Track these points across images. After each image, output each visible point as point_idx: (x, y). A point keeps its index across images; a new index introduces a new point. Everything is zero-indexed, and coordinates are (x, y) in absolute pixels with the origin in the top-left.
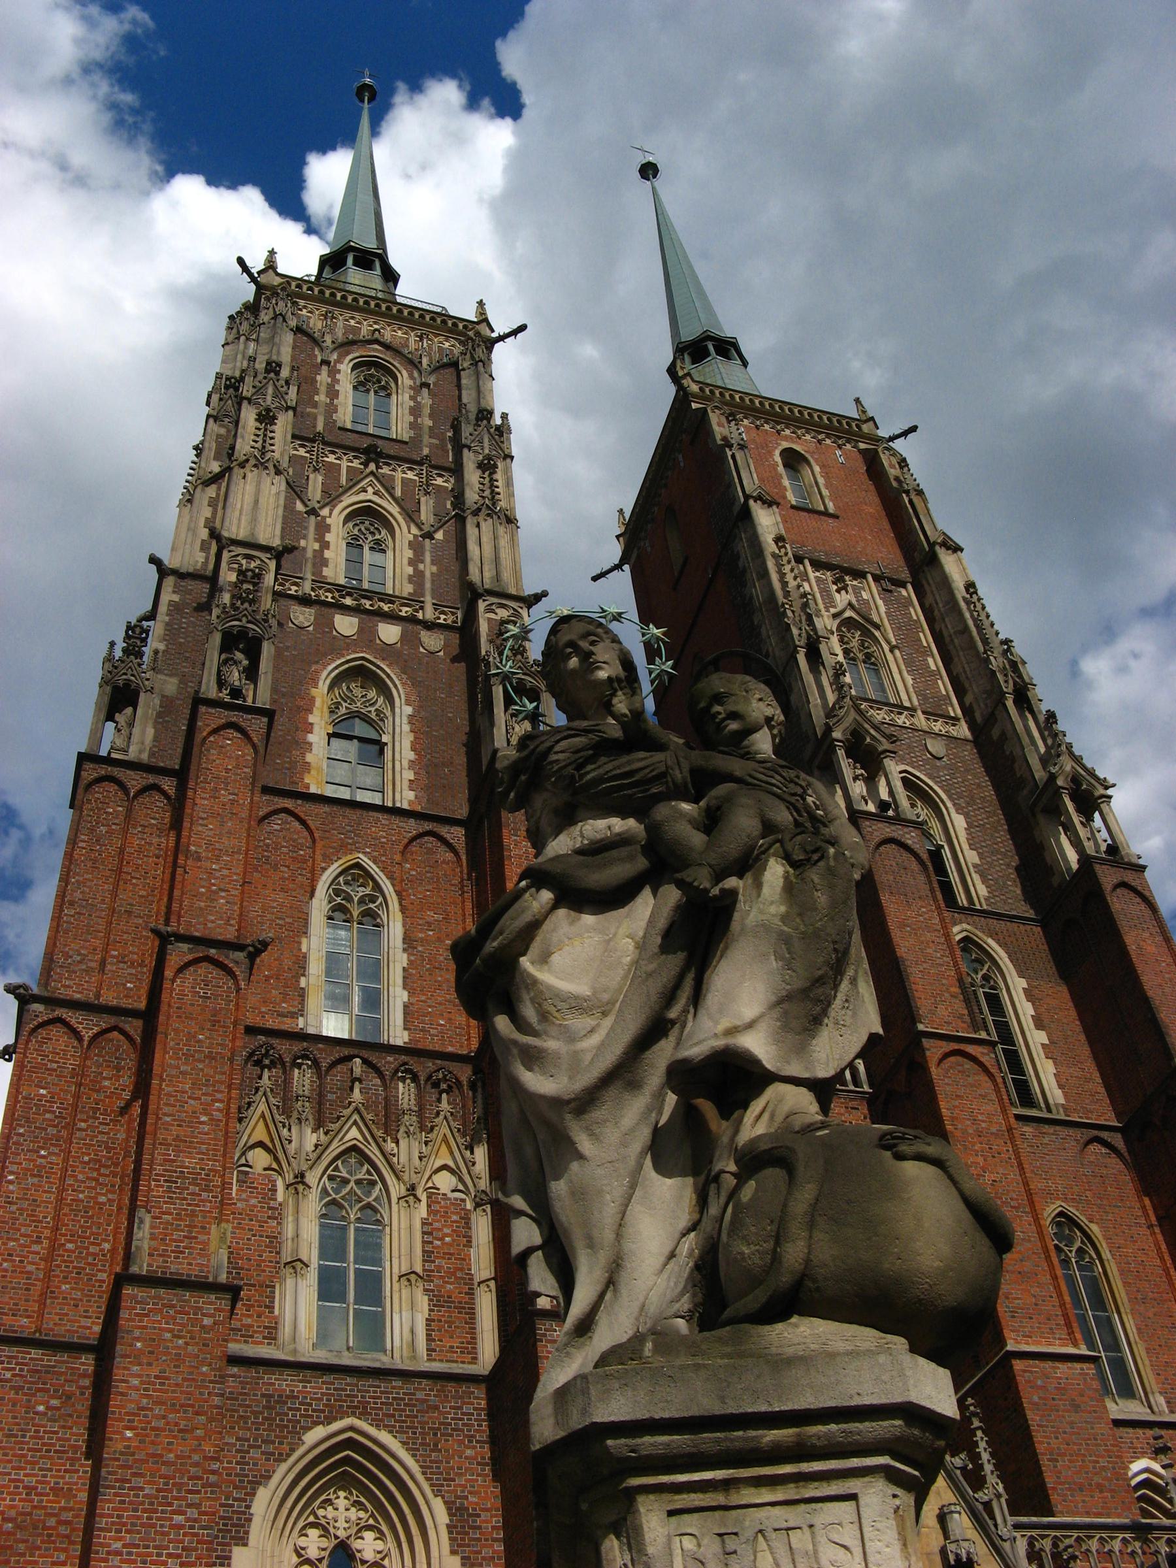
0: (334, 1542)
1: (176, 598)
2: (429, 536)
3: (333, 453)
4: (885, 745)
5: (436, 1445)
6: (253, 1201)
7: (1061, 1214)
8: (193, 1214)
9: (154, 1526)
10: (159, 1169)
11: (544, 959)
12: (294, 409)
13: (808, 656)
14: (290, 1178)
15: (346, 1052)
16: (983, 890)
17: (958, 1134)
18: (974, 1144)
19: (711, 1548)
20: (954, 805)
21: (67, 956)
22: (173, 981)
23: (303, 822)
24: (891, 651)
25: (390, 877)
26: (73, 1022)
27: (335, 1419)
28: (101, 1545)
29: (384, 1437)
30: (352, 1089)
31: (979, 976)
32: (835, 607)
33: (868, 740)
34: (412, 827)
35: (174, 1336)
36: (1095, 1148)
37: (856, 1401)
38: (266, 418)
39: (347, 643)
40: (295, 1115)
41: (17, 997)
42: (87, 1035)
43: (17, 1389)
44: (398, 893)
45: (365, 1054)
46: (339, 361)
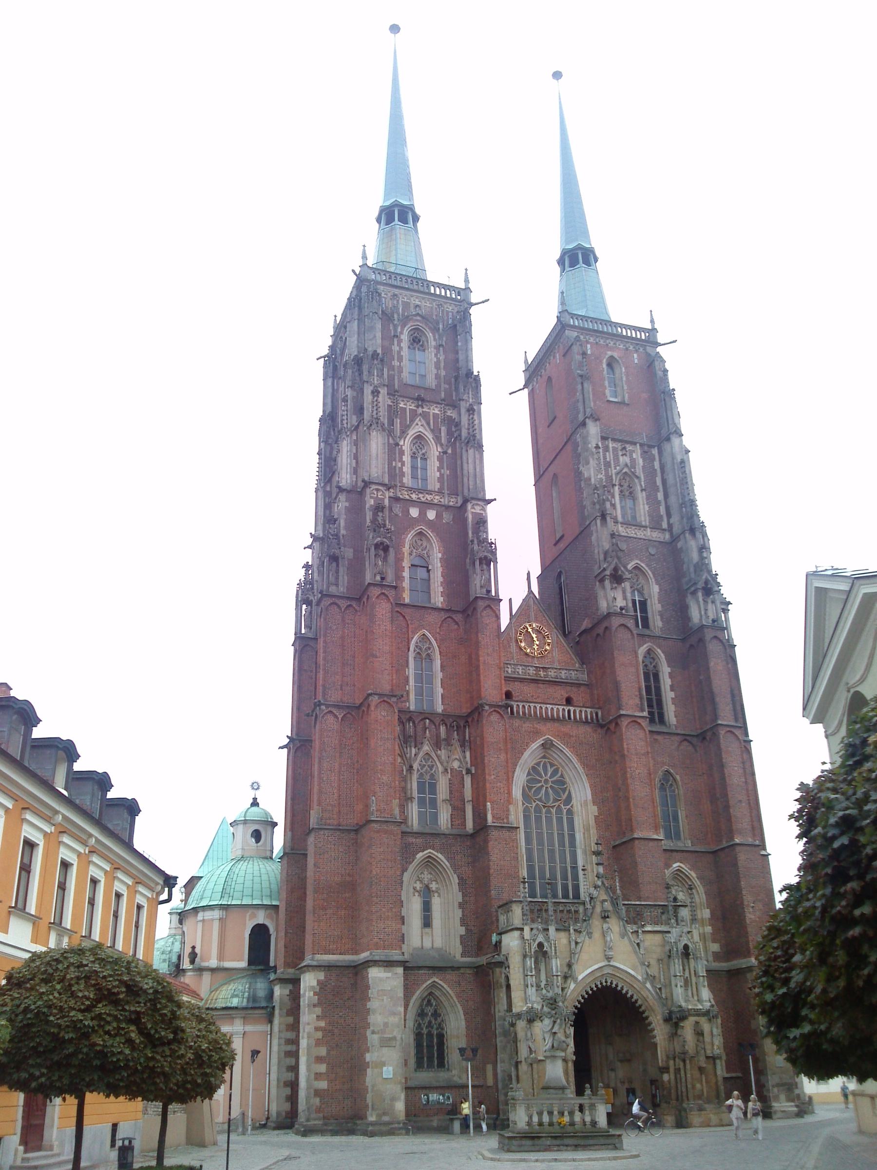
3: (403, 401)
12: (387, 386)
13: (601, 520)
14: (408, 767)
16: (660, 624)
20: (656, 580)
24: (642, 490)
30: (425, 732)
32: (619, 466)
34: (443, 615)
36: (686, 743)
38: (375, 393)
39: (415, 522)
42: (340, 717)
46: (401, 333)
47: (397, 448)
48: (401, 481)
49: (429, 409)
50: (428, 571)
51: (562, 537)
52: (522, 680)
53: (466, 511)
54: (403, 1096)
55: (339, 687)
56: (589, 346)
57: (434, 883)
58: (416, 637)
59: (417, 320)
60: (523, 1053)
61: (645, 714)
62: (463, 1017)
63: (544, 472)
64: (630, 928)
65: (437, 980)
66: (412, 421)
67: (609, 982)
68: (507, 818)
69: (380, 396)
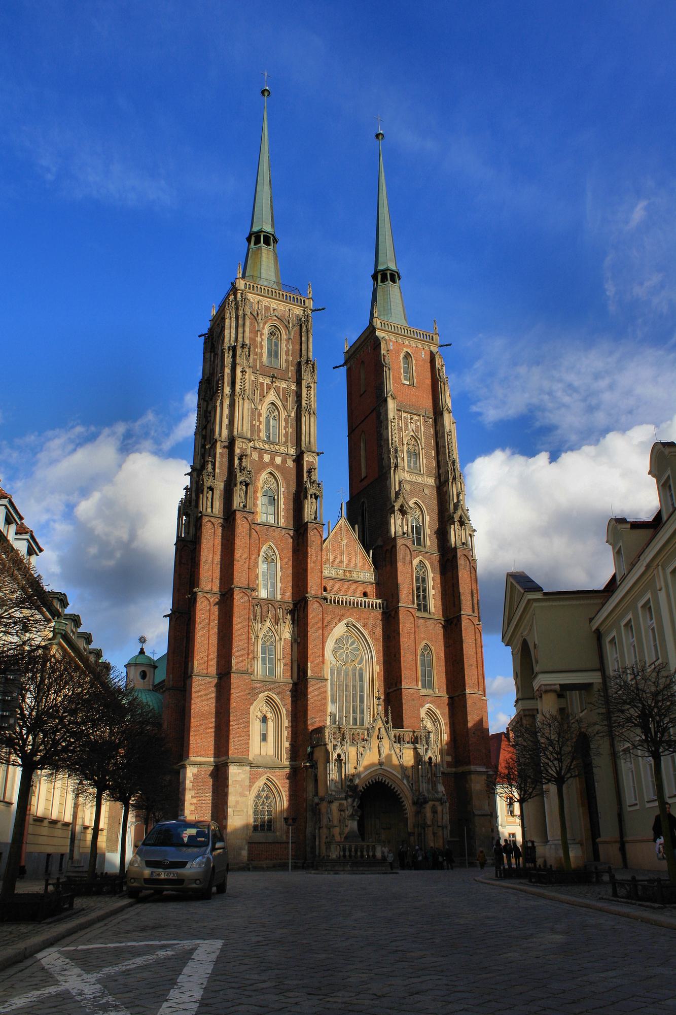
1: (221, 451)
15: (267, 602)
32: (408, 430)
46: (263, 328)
48: (258, 436)
51: (366, 477)
52: (334, 579)
53: (303, 459)
54: (246, 847)
56: (391, 344)
59: (275, 320)
60: (324, 821)
61: (415, 606)
63: (356, 428)
64: (397, 745)
65: (269, 775)
67: (380, 778)
68: (321, 673)
69: (247, 374)
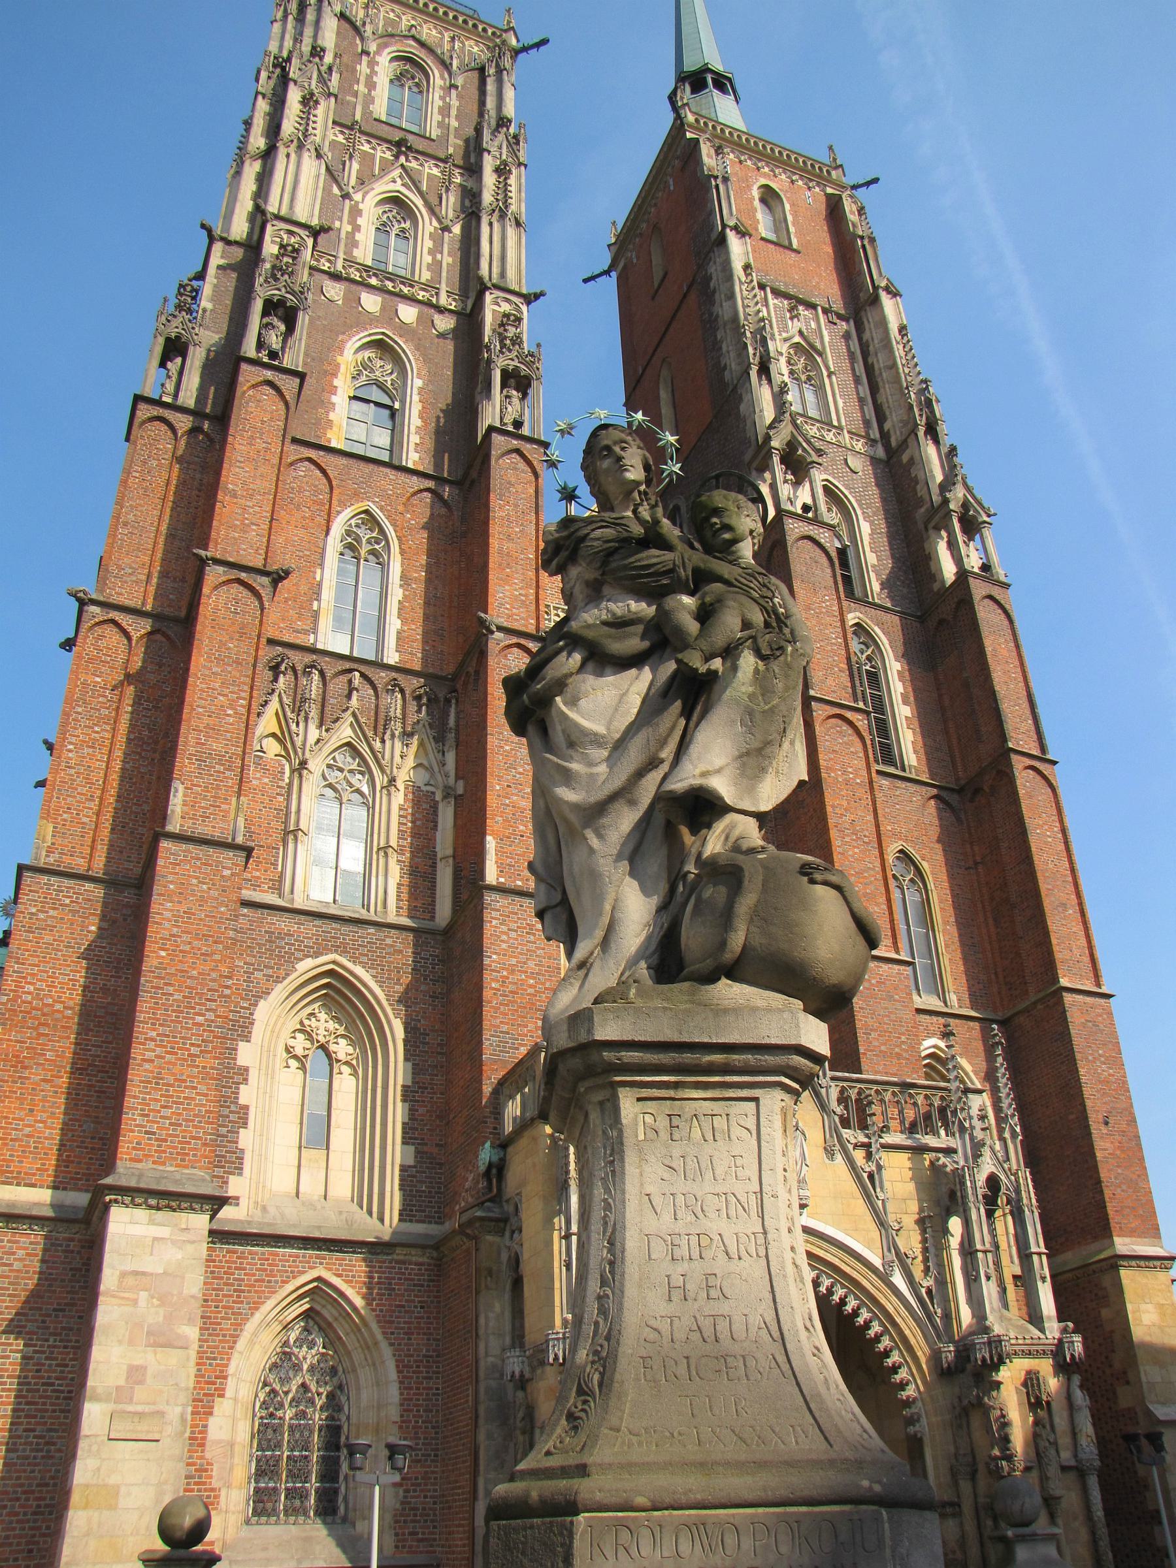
0: (316, 1045)
2: (446, 229)
4: (815, 458)
5: (398, 980)
6: (266, 780)
7: (901, 851)
8: (218, 788)
9: (180, 1022)
10: (192, 750)
11: (573, 702)
15: (348, 665)
17: (829, 780)
18: (841, 790)
19: (663, 1123)
20: (863, 513)
21: (120, 568)
22: (209, 597)
23: (324, 472)
25: (394, 525)
26: (124, 624)
27: (322, 954)
28: (140, 1033)
29: (359, 970)
30: (349, 696)
31: (864, 656)
33: (800, 452)
34: (416, 483)
35: (200, 882)
37: (767, 1041)
39: (371, 319)
40: (303, 713)
41: (78, 600)
43: (74, 912)
44: (399, 538)
45: (363, 668)
47: (347, 201)
48: (348, 252)
49: (422, 165)
50: (393, 416)
55: (144, 578)
57: (342, 1042)
58: (348, 513)
62: (393, 1374)
66: (384, 170)
